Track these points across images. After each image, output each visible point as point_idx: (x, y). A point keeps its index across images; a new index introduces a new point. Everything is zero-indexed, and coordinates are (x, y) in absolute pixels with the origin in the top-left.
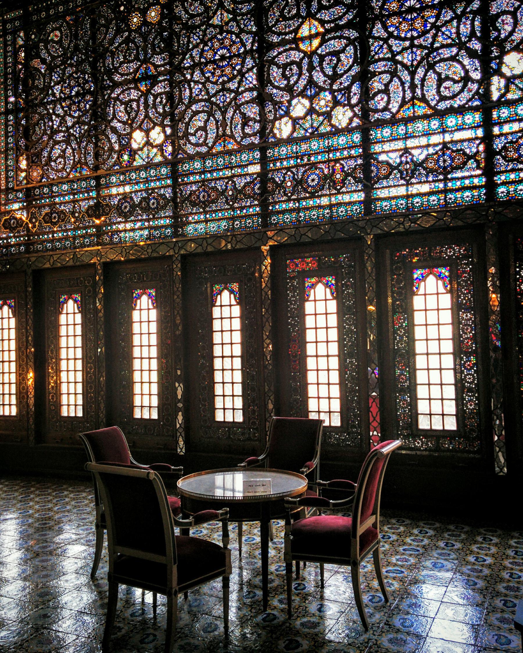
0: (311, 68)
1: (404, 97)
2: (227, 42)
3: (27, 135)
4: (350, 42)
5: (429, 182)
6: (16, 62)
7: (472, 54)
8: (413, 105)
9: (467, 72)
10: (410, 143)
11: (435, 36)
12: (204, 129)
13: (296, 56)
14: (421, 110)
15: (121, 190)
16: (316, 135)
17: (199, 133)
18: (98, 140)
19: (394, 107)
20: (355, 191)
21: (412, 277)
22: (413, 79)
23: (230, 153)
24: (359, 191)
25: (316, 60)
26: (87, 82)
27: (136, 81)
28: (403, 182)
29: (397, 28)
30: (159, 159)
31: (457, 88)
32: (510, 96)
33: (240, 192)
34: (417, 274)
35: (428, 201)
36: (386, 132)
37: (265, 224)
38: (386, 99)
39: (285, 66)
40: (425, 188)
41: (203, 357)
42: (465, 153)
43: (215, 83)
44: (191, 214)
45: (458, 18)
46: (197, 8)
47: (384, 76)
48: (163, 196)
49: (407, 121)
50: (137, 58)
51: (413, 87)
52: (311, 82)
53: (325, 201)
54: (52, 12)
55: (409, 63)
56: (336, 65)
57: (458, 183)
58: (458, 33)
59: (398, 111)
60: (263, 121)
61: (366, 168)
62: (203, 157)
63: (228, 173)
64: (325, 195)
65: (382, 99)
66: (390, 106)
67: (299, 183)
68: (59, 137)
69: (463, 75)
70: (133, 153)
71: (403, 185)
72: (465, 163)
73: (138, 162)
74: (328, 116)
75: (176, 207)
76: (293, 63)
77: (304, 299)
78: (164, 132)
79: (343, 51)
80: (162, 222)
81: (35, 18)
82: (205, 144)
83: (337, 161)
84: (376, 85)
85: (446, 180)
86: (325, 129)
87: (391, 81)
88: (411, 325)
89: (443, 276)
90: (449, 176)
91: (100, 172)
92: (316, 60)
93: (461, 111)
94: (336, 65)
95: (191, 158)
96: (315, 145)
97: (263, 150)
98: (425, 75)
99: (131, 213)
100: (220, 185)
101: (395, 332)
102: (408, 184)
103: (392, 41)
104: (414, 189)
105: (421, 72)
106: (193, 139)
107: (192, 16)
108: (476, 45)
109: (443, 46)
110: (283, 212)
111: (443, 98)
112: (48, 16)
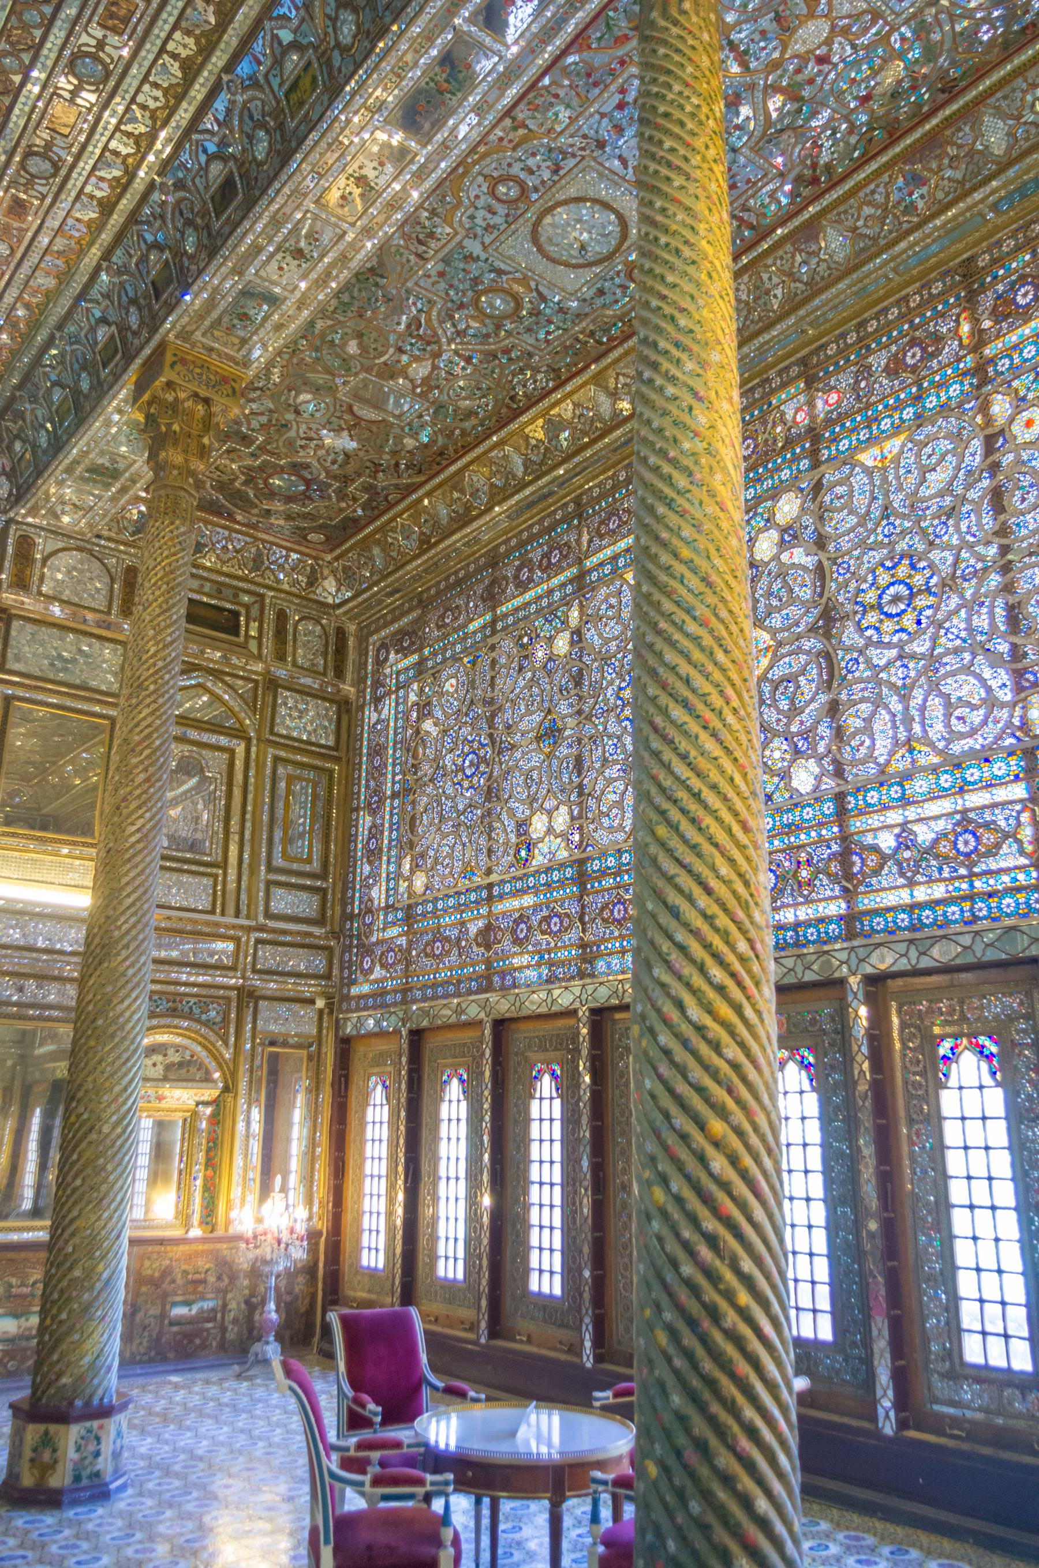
1: (895, 737)
5: (945, 880)
7: (995, 661)
8: (911, 750)
9: (989, 690)
10: (912, 813)
11: (934, 640)
12: (619, 804)
15: (516, 903)
17: (615, 811)
18: (491, 829)
20: (831, 898)
21: (937, 1052)
22: (907, 708)
24: (836, 898)
25: (767, 688)
26: (483, 746)
28: (901, 881)
29: (877, 629)
30: (562, 854)
31: (977, 717)
34: (944, 1048)
35: (945, 913)
38: (868, 743)
40: (939, 891)
42: (997, 830)
44: (604, 940)
47: (863, 706)
51: (908, 720)
54: (448, 654)
55: (900, 683)
56: (794, 693)
57: (1006, 878)
58: (970, 629)
59: (888, 762)
64: (788, 906)
65: (862, 744)
66: (876, 753)
68: (447, 827)
69: (983, 695)
71: (903, 886)
72: (998, 846)
73: (539, 860)
74: (785, 775)
78: (571, 812)
79: (803, 672)
87: (874, 713)
88: (940, 1148)
89: (986, 1052)
90: (976, 870)
91: (494, 878)
94: (794, 693)
98: (925, 700)
102: (911, 884)
103: (873, 652)
104: (921, 894)
105: (918, 695)
106: (606, 821)
107: (607, 641)
109: (947, 652)
112: (445, 660)
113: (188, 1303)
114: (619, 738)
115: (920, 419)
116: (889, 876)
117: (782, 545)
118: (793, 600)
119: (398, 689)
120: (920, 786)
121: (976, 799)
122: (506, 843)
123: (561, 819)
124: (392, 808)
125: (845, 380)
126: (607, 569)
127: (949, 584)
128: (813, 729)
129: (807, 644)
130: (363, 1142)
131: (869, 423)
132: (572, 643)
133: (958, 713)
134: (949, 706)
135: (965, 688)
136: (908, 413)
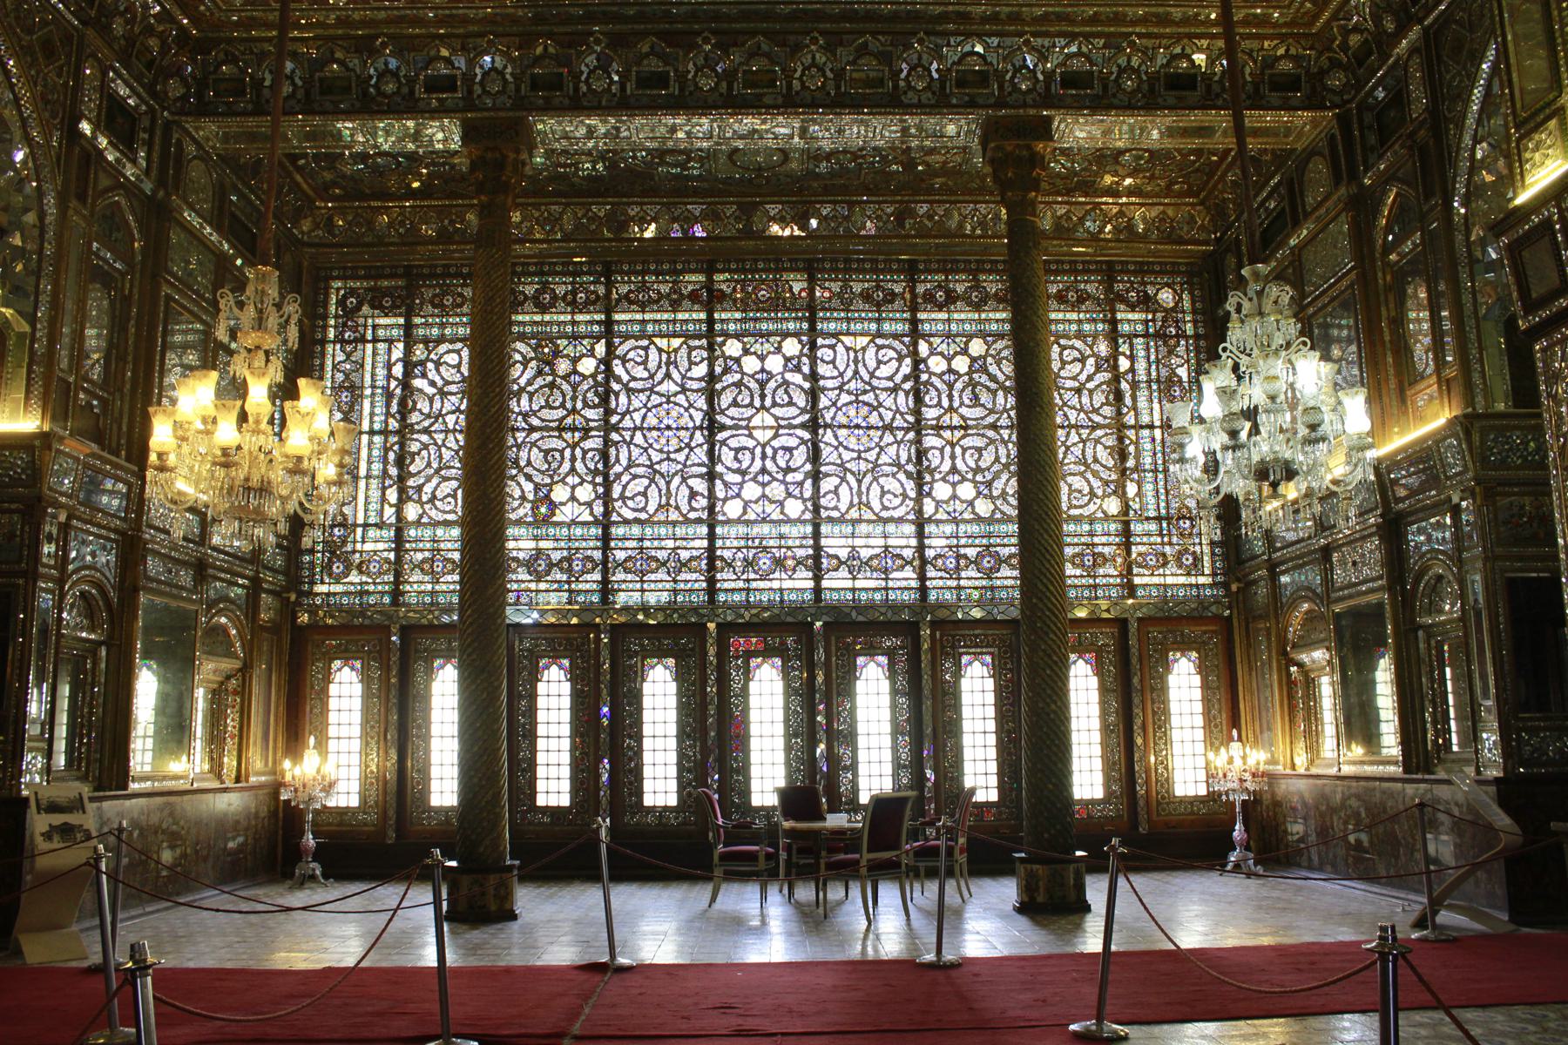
0: (764, 456)
2: (674, 414)
6: (389, 376)
7: (909, 475)
10: (858, 542)
11: (879, 455)
13: (751, 443)
14: (868, 515)
19: (843, 507)
23: (674, 524)
25: (769, 451)
27: (560, 429)
32: (938, 516)
33: (684, 565)
36: (836, 529)
37: (712, 600)
39: (737, 450)
41: (630, 737)
43: (661, 451)
45: (899, 443)
46: (640, 372)
48: (589, 559)
49: (854, 522)
50: (563, 405)
52: (764, 471)
53: (776, 585)
61: (817, 558)
63: (670, 544)
67: (748, 563)
70: (553, 506)
74: (781, 504)
75: (605, 572)
76: (745, 448)
77: (748, 677)
80: (587, 586)
81: (421, 332)
82: (643, 509)
83: (789, 548)
84: (827, 485)
85: (887, 579)
86: (776, 516)
92: (769, 451)
93: (900, 520)
95: (626, 522)
96: (765, 529)
97: (712, 528)
99: (548, 573)
100: (662, 555)
101: (839, 713)
102: (854, 578)
104: (859, 584)
107: (634, 379)
108: (910, 468)
110: (733, 590)
111: (885, 508)
113: (234, 839)
114: (646, 450)
115: (879, 334)
116: (843, 572)
118: (791, 403)
119: (375, 340)
120: (863, 528)
121: (891, 542)
123: (585, 493)
124: (370, 443)
125: (836, 287)
126: (637, 328)
127: (888, 428)
128: (801, 484)
129: (800, 432)
131: (848, 320)
132: (597, 367)
133: (889, 496)
134: (883, 493)
135: (891, 484)
136: (873, 326)
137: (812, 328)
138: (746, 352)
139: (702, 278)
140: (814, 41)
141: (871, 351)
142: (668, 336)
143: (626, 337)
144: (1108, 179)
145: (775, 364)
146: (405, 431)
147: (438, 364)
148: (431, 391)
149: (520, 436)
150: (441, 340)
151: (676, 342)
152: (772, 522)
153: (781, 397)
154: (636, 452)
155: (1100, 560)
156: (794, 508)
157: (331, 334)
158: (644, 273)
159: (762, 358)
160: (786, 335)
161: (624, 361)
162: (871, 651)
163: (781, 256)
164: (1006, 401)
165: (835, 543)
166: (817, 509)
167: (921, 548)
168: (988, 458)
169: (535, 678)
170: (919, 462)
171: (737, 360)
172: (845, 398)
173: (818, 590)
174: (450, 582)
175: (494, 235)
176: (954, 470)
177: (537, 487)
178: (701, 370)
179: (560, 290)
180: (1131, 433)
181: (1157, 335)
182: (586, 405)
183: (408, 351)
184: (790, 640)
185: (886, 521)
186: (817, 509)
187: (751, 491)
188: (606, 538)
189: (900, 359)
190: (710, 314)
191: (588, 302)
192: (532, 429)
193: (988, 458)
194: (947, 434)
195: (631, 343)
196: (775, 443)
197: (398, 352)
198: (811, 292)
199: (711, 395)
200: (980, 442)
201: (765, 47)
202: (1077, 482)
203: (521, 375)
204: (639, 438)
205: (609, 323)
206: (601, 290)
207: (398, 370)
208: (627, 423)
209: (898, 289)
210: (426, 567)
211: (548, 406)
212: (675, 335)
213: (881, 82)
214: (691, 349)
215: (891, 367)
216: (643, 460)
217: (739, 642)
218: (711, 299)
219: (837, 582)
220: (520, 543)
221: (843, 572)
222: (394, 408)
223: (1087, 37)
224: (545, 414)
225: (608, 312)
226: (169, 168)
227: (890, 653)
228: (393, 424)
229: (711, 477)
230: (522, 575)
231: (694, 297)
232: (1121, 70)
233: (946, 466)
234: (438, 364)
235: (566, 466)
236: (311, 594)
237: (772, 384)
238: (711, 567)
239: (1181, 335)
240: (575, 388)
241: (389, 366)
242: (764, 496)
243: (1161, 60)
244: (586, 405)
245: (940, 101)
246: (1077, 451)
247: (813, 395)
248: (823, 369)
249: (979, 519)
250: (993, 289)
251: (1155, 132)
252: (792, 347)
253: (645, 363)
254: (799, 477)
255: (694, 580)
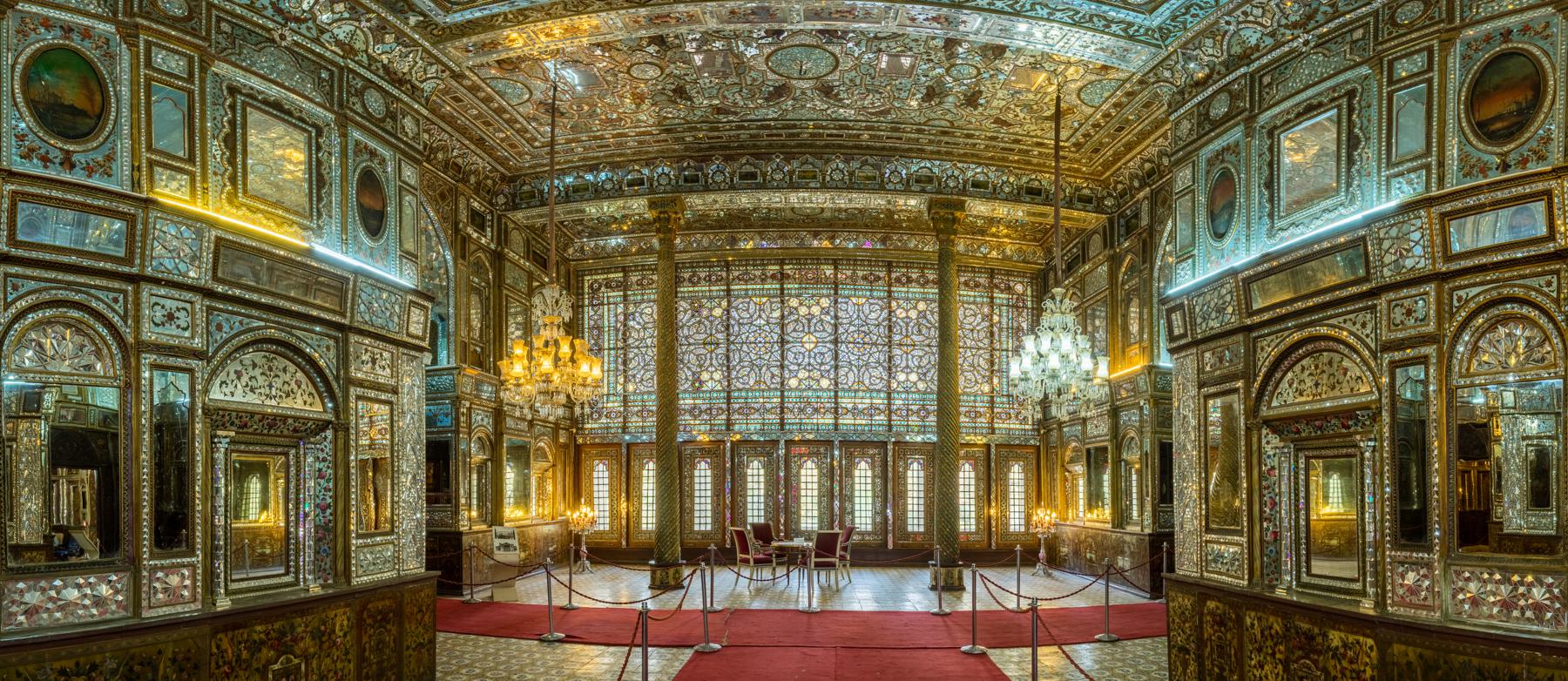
3: (625, 363)
4: (830, 350)
10: (857, 401)
13: (803, 350)
16: (809, 388)
27: (704, 344)
48: (721, 408)
50: (705, 332)
52: (809, 364)
60: (782, 376)
61: (836, 409)
62: (747, 390)
70: (701, 383)
73: (705, 388)
77: (800, 467)
84: (842, 372)
100: (755, 406)
116: (850, 416)
117: (821, 313)
118: (824, 330)
120: (861, 394)
122: (687, 379)
123: (717, 376)
127: (875, 344)
130: (592, 485)
135: (875, 373)
137: (836, 293)
138: (801, 304)
139: (777, 267)
140: (838, 157)
141: (866, 307)
142: (760, 296)
143: (738, 297)
144: (994, 230)
145: (816, 310)
146: (626, 348)
147: (641, 314)
148: (637, 327)
149: (684, 348)
150: (643, 301)
151: (764, 300)
152: (815, 390)
153: (819, 326)
154: (743, 355)
155: (978, 414)
156: (825, 383)
157: (586, 302)
158: (746, 265)
159: (809, 307)
160: (823, 296)
161: (737, 309)
162: (863, 456)
163: (818, 258)
164: (934, 333)
165: (846, 402)
166: (836, 384)
167: (889, 404)
168: (925, 361)
169: (693, 467)
170: (890, 361)
171: (796, 309)
172: (853, 328)
173: (836, 425)
174: (652, 421)
175: (668, 251)
176: (907, 367)
177: (694, 374)
178: (777, 314)
179: (703, 275)
180: (997, 353)
181: (1013, 306)
182: (717, 331)
183: (626, 307)
184: (822, 450)
185: (872, 391)
186: (836, 384)
187: (802, 374)
188: (729, 398)
189: (882, 310)
190: (782, 285)
191: (717, 280)
192: (690, 344)
193: (925, 361)
194: (905, 348)
195: (740, 300)
196: (816, 351)
197: (620, 310)
198: (836, 275)
199: (783, 327)
200: (921, 353)
201: (810, 160)
202: (970, 376)
203: (683, 317)
204: (745, 348)
205: (728, 291)
206: (724, 274)
207: (621, 318)
208: (739, 339)
209: (882, 275)
210: (640, 413)
211: (698, 333)
212: (763, 296)
213: (874, 178)
214: (771, 303)
215: (876, 314)
216: (747, 359)
217: (796, 450)
218: (782, 277)
219: (846, 421)
220: (686, 402)
221: (850, 416)
222: (620, 336)
223: (987, 165)
224: (697, 337)
225: (728, 285)
226: (503, 237)
227: (872, 457)
228: (620, 344)
229: (782, 367)
230: (687, 417)
231: (773, 277)
232: (1003, 183)
233: (903, 365)
234: (641, 314)
235: (708, 362)
236: (582, 429)
237: (814, 321)
238: (782, 412)
239: (1025, 307)
240: (711, 322)
241: (616, 315)
242: (809, 377)
243: (1024, 179)
244: (717, 331)
245: (907, 190)
246: (970, 360)
247: (836, 326)
248: (840, 314)
249: (918, 391)
250: (931, 277)
251: (1019, 212)
252: (825, 302)
253: (747, 310)
254: (828, 367)
255: (773, 418)
